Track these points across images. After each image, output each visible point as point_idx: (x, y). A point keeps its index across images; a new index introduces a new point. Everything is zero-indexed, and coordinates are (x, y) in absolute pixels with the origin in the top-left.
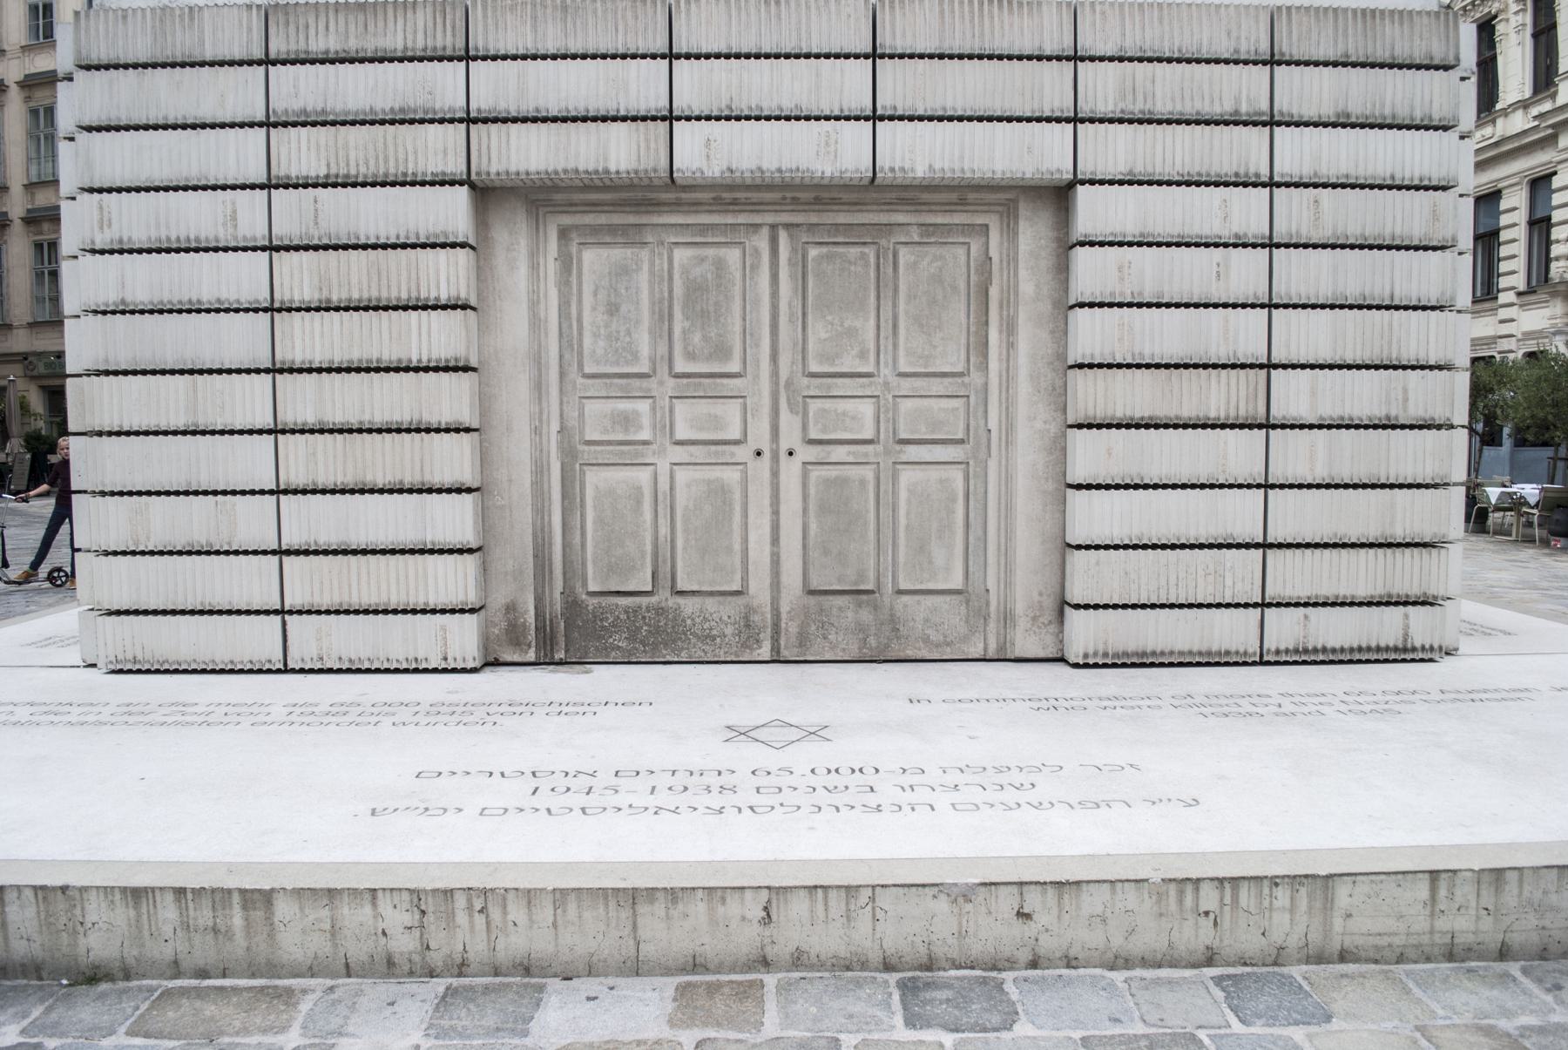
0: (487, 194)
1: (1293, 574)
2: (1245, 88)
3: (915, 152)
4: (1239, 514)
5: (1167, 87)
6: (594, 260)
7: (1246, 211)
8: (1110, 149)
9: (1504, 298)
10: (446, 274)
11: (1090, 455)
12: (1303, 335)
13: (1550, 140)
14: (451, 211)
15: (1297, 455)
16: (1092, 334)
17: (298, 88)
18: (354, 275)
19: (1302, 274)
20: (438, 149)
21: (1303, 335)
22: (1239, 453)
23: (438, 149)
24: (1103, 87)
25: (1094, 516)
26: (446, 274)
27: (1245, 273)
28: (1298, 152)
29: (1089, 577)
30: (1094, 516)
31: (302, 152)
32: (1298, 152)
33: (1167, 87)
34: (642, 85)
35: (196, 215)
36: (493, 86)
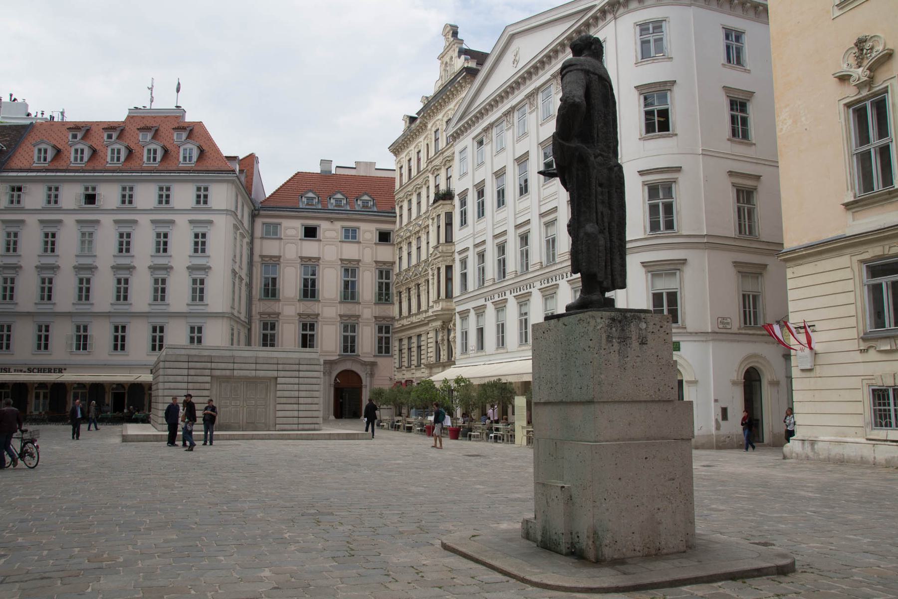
0: (212, 376)
1: (301, 420)
2: (296, 367)
3: (261, 374)
4: (296, 414)
5: (287, 367)
6: (223, 385)
7: (296, 381)
8: (282, 374)
9: (413, 367)
10: (208, 386)
11: (279, 407)
12: (302, 394)
13: (427, 324)
14: (208, 379)
15: (302, 407)
16: (279, 394)
17: (192, 365)
18: (197, 386)
19: (302, 387)
20: (208, 372)
21: (302, 394)
22: (295, 407)
23: (208, 372)
24: (280, 367)
25: (279, 414)
26: (208, 386)
27: (296, 387)
28: (302, 374)
29: (279, 421)
30: (279, 414)
31: (192, 372)
32: (302, 374)
33: (287, 367)
34: (231, 366)
35: (179, 378)
36: (214, 365)
